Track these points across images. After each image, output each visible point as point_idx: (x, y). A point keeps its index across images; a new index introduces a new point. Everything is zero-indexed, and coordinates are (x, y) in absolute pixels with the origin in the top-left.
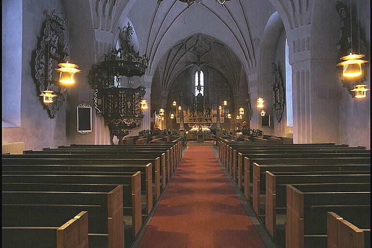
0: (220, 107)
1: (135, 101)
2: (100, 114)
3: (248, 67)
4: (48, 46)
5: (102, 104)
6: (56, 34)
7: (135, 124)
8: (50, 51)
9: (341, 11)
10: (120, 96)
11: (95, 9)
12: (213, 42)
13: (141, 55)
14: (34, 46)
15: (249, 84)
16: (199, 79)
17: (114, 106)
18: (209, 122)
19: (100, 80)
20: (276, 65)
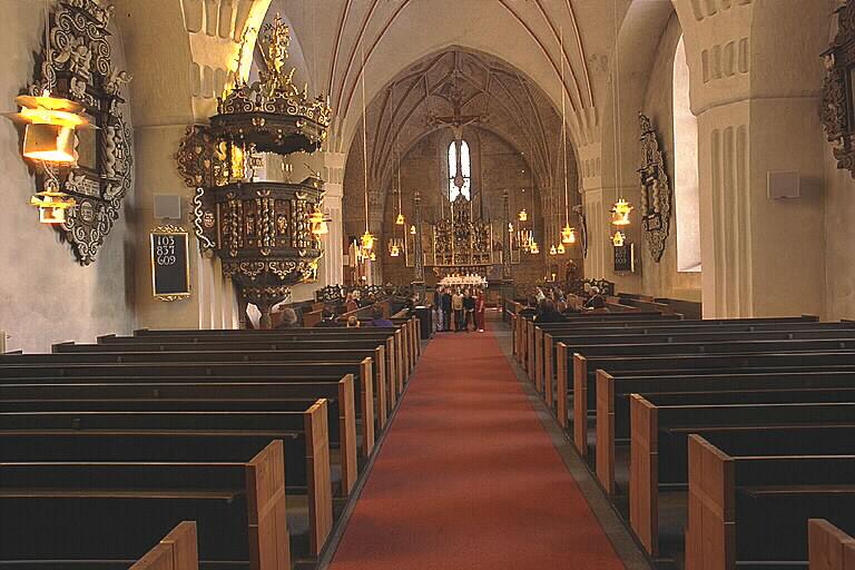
1: (297, 216)
5: (216, 224)
6: (86, 44)
12: (491, 69)
15: (582, 168)
16: (459, 158)
17: (244, 227)
20: (648, 120)
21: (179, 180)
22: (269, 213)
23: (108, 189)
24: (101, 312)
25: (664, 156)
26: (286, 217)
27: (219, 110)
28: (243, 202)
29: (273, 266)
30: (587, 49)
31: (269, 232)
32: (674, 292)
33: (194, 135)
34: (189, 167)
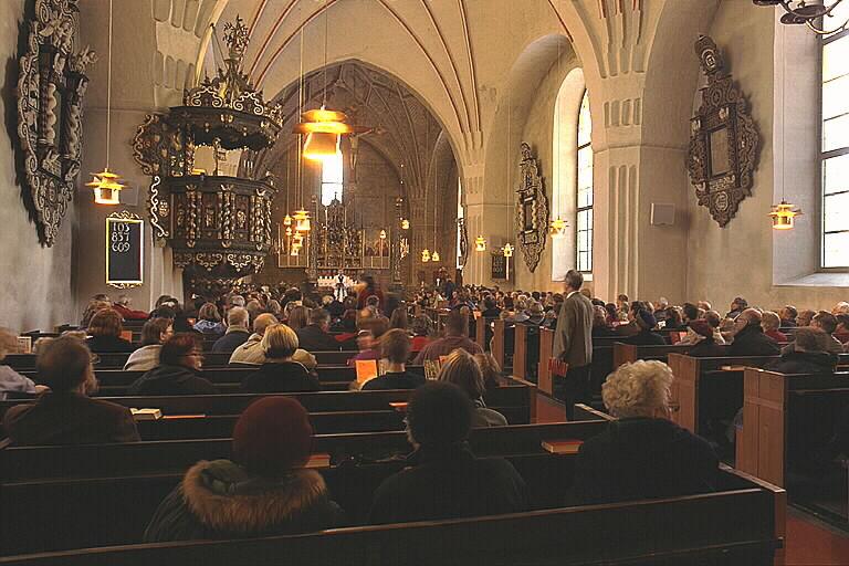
0: (383, 232)
1: (255, 211)
5: (169, 214)
10: (221, 196)
18: (355, 266)
19: (165, 152)
24: (53, 298)
25: (543, 180)
26: (244, 211)
27: (185, 101)
28: (204, 193)
29: (230, 257)
30: (479, 81)
31: (229, 226)
33: (153, 123)
34: (149, 156)
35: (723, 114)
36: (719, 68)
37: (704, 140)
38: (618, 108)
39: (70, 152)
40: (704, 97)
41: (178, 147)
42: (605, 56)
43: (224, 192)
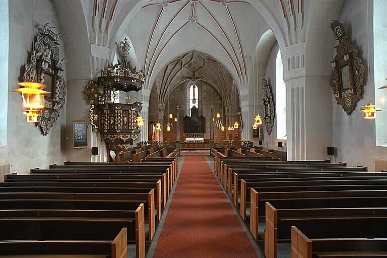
1: (131, 117)
2: (96, 130)
3: (240, 83)
4: (40, 61)
5: (98, 119)
7: (132, 139)
8: (42, 65)
9: (337, 29)
11: (91, 25)
13: (138, 69)
14: (23, 60)
16: (193, 93)
17: (110, 121)
19: (96, 95)
20: (266, 81)
21: (84, 102)
22: (120, 116)
23: (56, 105)
24: (52, 154)
29: (121, 136)
31: (120, 123)
32: (275, 147)
34: (88, 97)
35: (346, 58)
36: (344, 35)
37: (338, 72)
38: (299, 59)
39: (55, 98)
40: (337, 51)
41: (102, 92)
42: (287, 37)
43: (117, 110)
